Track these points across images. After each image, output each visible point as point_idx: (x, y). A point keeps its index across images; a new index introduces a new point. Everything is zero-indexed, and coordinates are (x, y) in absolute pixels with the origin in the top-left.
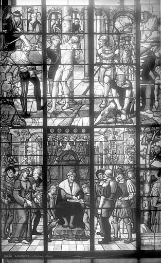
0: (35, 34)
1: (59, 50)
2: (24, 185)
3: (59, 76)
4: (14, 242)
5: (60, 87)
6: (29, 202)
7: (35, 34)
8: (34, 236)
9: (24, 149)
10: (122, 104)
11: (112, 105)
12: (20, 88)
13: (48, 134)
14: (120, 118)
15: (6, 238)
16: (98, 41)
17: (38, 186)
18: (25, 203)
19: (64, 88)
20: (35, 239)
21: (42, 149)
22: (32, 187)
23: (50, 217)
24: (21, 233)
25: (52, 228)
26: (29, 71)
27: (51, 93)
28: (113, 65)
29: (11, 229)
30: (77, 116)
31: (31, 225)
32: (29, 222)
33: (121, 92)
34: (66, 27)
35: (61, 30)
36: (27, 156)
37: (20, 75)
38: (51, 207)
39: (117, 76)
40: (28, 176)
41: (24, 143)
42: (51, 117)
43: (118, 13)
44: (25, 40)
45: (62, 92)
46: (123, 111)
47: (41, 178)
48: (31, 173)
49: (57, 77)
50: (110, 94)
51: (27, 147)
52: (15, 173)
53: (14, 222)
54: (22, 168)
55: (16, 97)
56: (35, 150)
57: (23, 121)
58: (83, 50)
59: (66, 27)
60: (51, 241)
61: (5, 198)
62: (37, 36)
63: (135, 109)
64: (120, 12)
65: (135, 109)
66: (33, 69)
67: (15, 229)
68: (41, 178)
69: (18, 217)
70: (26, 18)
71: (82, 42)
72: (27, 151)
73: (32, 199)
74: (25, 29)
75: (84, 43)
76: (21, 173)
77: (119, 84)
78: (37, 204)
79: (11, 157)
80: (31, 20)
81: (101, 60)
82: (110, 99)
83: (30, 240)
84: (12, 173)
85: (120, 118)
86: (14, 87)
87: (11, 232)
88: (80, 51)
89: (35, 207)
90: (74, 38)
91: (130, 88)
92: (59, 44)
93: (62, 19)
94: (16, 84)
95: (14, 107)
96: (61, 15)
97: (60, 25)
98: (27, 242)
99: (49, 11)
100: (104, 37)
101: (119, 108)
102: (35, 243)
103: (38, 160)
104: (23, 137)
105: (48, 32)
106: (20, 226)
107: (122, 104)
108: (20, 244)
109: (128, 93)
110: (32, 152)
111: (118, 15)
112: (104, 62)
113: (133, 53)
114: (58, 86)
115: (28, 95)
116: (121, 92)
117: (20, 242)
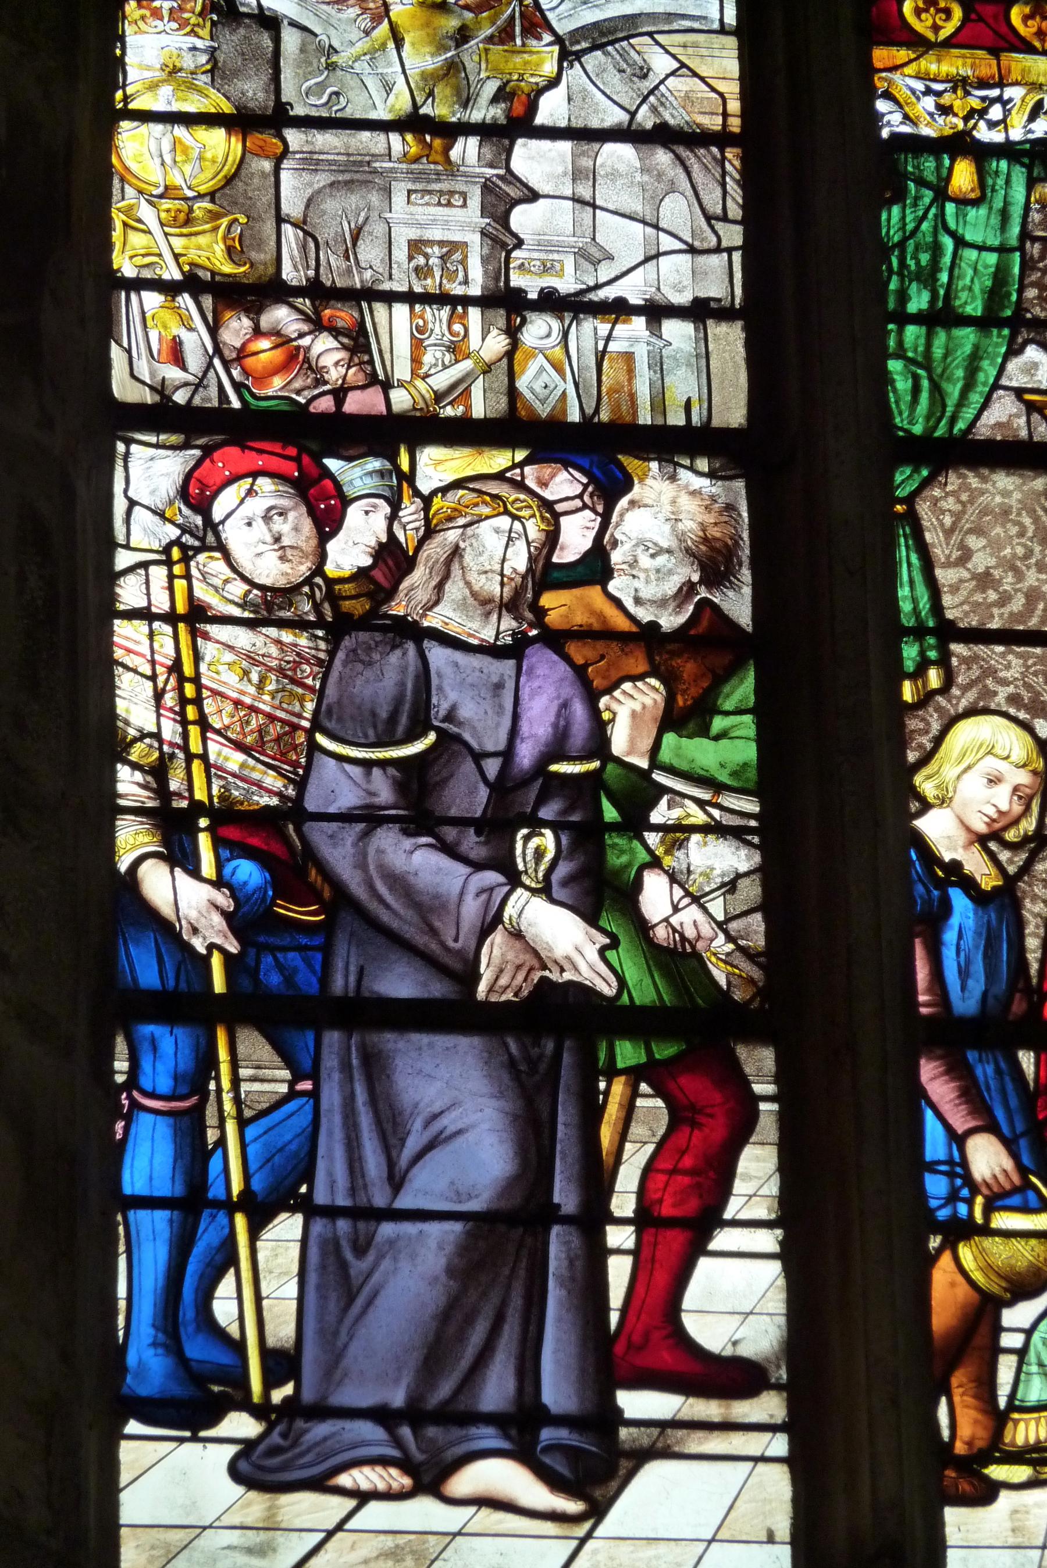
2: (461, 690)
4: (320, 1484)
6: (562, 935)
8: (638, 1404)
9: (464, 223)
13: (881, 55)
15: (189, 1412)
17: (685, 716)
18: (497, 943)
20: (662, 1442)
21: (733, 235)
22: (600, 729)
23: (958, 1139)
24: (434, 1357)
25: (984, 1311)
29: (282, 1292)
31: (597, 1254)
32: (565, 1195)
36: (507, 304)
38: (966, 1001)
40: (546, 574)
41: (467, 150)
47: (738, 605)
48: (576, 537)
51: (503, 198)
52: (328, 523)
53: (329, 1184)
54: (437, 465)
56: (624, 239)
60: (986, 1493)
61: (180, 856)
67: (335, 1281)
68: (738, 605)
69: (391, 1126)
72: (502, 241)
73: (602, 894)
76: (430, 532)
78: (678, 960)
79: (281, 316)
83: (592, 1468)
84: (296, 527)
87: (282, 1329)
89: (644, 988)
98: (534, 1493)
102: (657, 1498)
103: (701, 374)
104: (453, 68)
106: (414, 1271)
108: (424, 1513)
110: (591, 255)
117: (429, 1479)
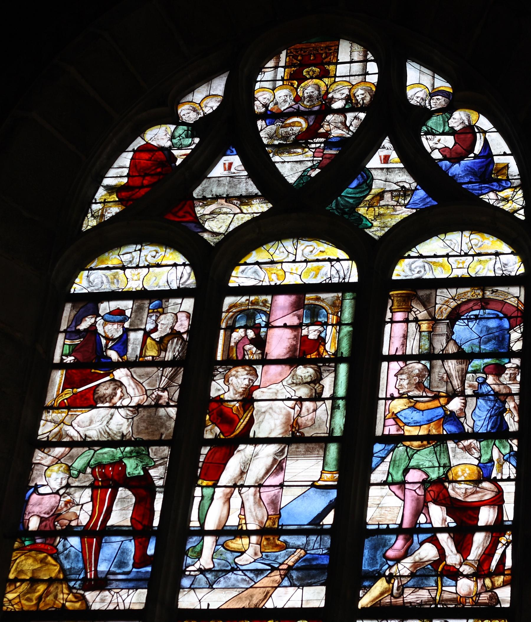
0: (163, 364)
1: (248, 400)
3: (237, 472)
5: (236, 501)
7: (164, 364)
10: (463, 547)
11: (427, 552)
12: (89, 507)
14: (453, 589)
16: (392, 380)
19: (249, 504)
26: (125, 461)
27: (202, 520)
28: (437, 441)
30: (286, 582)
33: (464, 518)
34: (279, 343)
35: (263, 353)
37: (93, 470)
39: (450, 467)
42: (191, 588)
43: (464, 303)
44: (126, 381)
45: (242, 515)
46: (466, 569)
49: (227, 477)
50: (422, 519)
55: (69, 531)
57: (83, 598)
58: (329, 403)
59: (279, 343)
62: (168, 371)
63: (509, 563)
64: (469, 301)
65: (509, 563)
66: (138, 455)
70: (143, 327)
71: (327, 382)
74: (133, 351)
75: (336, 382)
77: (457, 491)
80: (155, 330)
81: (400, 428)
82: (422, 537)
85: (453, 589)
86: (67, 503)
88: (319, 403)
90: (305, 372)
91: (497, 501)
92: (250, 390)
93: (269, 326)
94: (77, 495)
95: (56, 559)
96: (268, 315)
97: (260, 342)
99: (231, 307)
100: (416, 367)
101: (453, 558)
105: (219, 358)
107: (463, 547)
109: (486, 516)
111: (464, 308)
112: (410, 431)
113: (511, 405)
114: (228, 500)
115: (109, 523)
116: (464, 518)
